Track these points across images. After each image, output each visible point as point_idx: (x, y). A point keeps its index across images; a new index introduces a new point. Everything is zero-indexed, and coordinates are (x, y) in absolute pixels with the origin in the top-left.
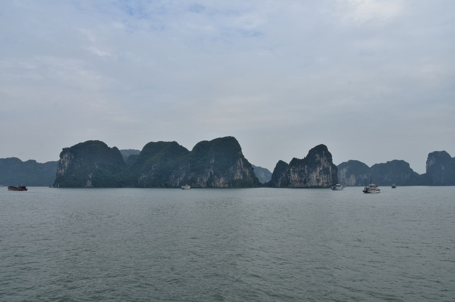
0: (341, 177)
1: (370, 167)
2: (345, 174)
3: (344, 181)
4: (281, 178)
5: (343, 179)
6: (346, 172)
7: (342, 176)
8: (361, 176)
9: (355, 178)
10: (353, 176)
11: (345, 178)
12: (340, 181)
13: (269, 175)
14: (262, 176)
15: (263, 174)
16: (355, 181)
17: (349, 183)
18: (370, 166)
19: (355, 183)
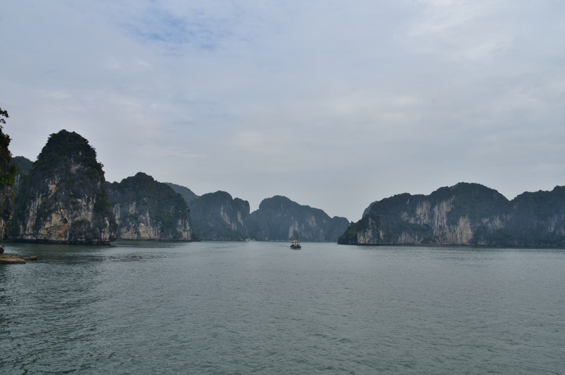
0: (436, 222)
1: (510, 199)
2: (444, 217)
3: (442, 233)
4: (39, 201)
5: (440, 227)
6: (449, 210)
7: (438, 219)
8: (485, 220)
9: (470, 225)
10: (466, 220)
11: (446, 226)
12: (434, 232)
13: (324, 221)
14: (310, 223)
15: (313, 219)
16: (470, 232)
17: (456, 238)
18: (510, 197)
19: (470, 238)
